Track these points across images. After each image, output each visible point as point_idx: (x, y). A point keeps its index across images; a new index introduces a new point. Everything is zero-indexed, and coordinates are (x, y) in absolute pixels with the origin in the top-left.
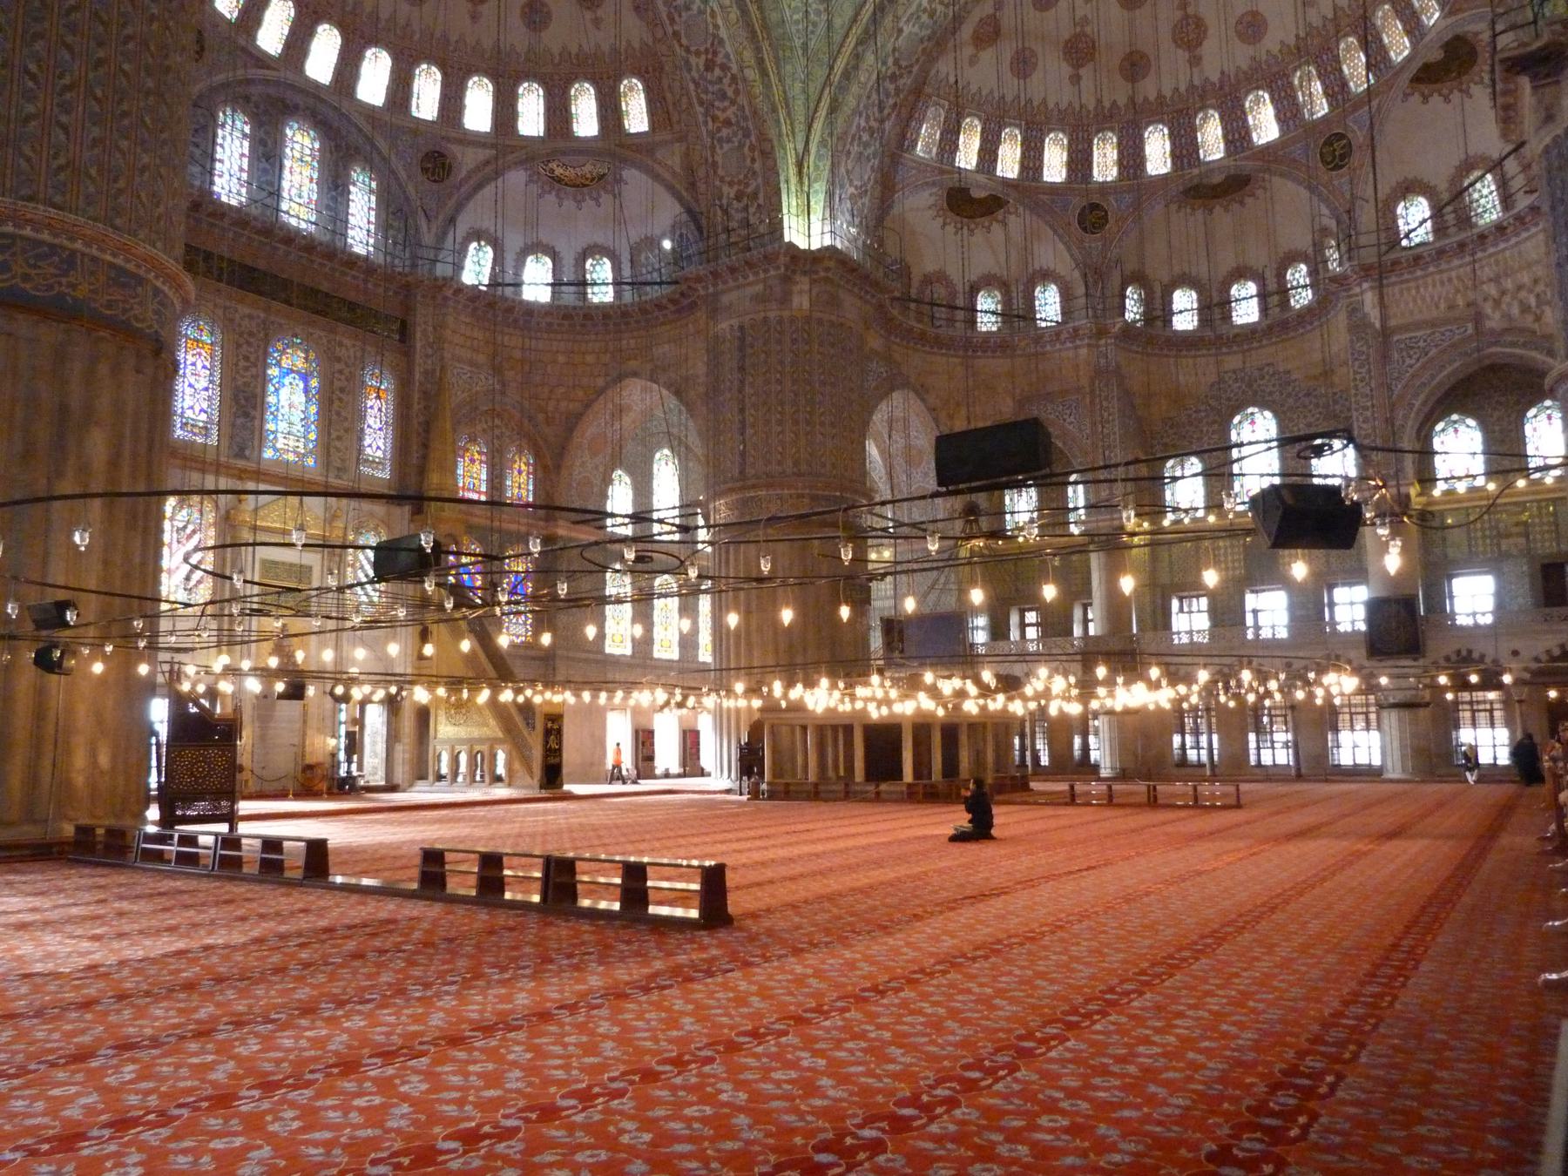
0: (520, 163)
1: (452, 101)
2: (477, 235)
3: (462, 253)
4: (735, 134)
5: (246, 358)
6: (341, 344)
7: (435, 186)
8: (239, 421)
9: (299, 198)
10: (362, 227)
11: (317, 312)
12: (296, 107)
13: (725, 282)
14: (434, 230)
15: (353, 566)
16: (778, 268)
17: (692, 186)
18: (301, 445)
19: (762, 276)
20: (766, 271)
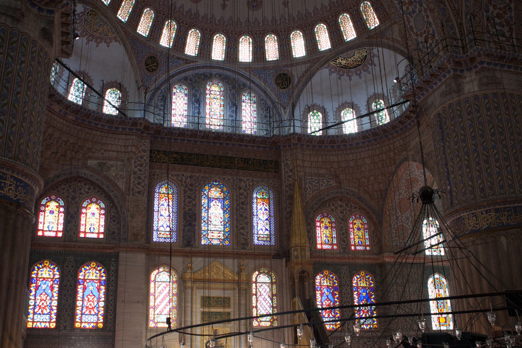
0: (321, 66)
1: (285, 47)
2: (309, 109)
3: (304, 121)
4: (416, 7)
5: (189, 197)
6: (241, 180)
7: (284, 91)
8: (187, 228)
9: (215, 115)
10: (249, 120)
11: (226, 167)
12: (211, 75)
13: (427, 91)
14: (288, 112)
15: (256, 295)
16: (449, 72)
17: (407, 44)
18: (221, 235)
19: (444, 80)
20: (444, 76)
